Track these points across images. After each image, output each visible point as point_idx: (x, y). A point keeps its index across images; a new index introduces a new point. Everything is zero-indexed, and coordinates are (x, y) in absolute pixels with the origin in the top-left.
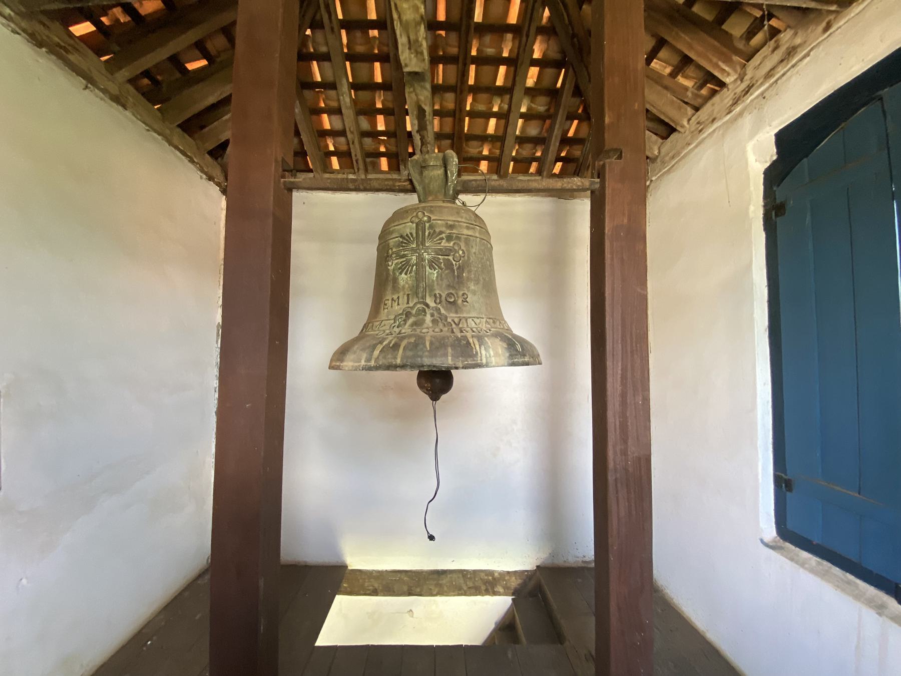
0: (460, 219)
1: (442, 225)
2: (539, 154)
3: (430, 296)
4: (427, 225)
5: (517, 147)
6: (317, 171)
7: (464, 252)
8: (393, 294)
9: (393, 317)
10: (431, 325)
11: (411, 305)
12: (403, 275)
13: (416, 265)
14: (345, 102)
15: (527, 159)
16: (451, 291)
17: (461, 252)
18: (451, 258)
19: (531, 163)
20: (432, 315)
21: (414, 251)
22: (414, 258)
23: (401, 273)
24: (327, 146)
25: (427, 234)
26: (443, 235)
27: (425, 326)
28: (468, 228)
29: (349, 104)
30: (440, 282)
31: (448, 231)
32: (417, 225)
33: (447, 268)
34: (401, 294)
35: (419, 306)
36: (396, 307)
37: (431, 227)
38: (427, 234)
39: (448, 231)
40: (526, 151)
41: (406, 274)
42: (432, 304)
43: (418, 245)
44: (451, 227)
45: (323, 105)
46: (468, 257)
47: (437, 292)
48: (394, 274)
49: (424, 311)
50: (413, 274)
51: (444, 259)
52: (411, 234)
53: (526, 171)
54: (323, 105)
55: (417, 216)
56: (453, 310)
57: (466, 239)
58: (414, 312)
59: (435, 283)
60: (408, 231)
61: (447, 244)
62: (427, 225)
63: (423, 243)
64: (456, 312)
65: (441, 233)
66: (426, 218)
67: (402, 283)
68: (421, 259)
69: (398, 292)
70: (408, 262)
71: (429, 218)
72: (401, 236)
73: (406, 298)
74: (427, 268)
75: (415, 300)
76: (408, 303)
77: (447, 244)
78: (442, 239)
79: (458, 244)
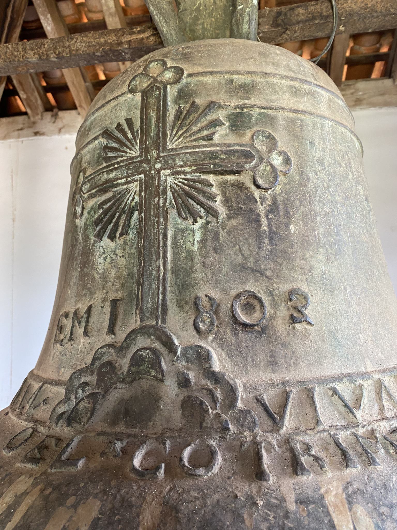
0: (268, 69)
1: (217, 88)
2: (384, 50)
3: (180, 306)
4: (172, 91)
5: (351, 44)
6: (81, 106)
7: (287, 161)
8: (79, 297)
9: (66, 375)
10: (177, 417)
11: (121, 335)
12: (106, 240)
13: (140, 207)
14: (108, 6)
15: (367, 57)
16: (251, 287)
17: (277, 161)
18: (245, 179)
19: (372, 64)
20: (184, 383)
21: (133, 166)
22: (134, 187)
23: (100, 236)
24: (97, 75)
25: (171, 114)
26: (221, 115)
27: (158, 423)
28: (295, 92)
29: (113, 10)
30: (212, 258)
31: (235, 102)
32: (145, 93)
33: (233, 212)
34: (99, 295)
35: (142, 342)
36: (82, 342)
37: (183, 95)
38: (171, 114)
39: (235, 102)
40: (365, 49)
41: (112, 237)
42: (183, 337)
43: (145, 150)
44: (246, 89)
45: (85, 20)
46: (301, 173)
47: (201, 294)
48: (86, 238)
49: (155, 363)
50: (132, 235)
51: (223, 185)
52: (129, 122)
53: (367, 76)
54: (85, 20)
55: (145, 74)
56: (262, 358)
57: (293, 121)
58: (124, 363)
59: (198, 260)
60: (121, 117)
61: (232, 139)
62: (172, 91)
63: (160, 142)
64: (273, 363)
65: (211, 106)
66: (169, 75)
67: (101, 264)
68: (151, 188)
69: (92, 294)
70: (118, 199)
71: (179, 72)
72: (107, 134)
73: (107, 309)
74: (173, 214)
75: (134, 323)
76: (111, 330)
77: (232, 139)
78: (215, 123)
79: (270, 137)
